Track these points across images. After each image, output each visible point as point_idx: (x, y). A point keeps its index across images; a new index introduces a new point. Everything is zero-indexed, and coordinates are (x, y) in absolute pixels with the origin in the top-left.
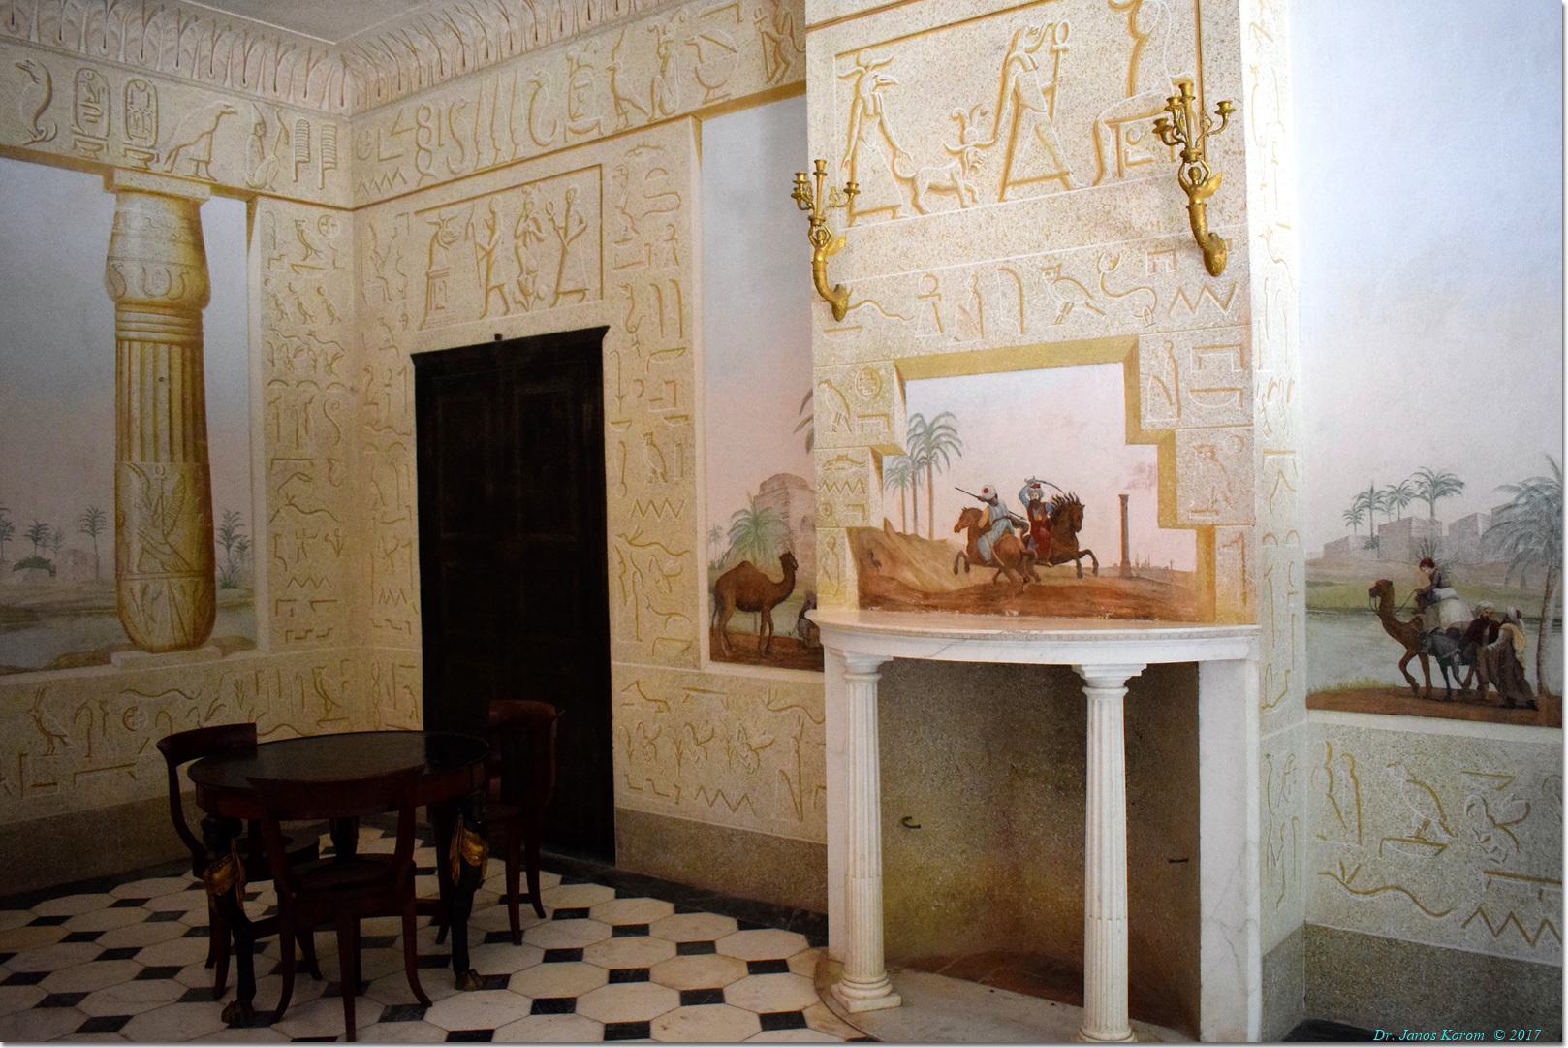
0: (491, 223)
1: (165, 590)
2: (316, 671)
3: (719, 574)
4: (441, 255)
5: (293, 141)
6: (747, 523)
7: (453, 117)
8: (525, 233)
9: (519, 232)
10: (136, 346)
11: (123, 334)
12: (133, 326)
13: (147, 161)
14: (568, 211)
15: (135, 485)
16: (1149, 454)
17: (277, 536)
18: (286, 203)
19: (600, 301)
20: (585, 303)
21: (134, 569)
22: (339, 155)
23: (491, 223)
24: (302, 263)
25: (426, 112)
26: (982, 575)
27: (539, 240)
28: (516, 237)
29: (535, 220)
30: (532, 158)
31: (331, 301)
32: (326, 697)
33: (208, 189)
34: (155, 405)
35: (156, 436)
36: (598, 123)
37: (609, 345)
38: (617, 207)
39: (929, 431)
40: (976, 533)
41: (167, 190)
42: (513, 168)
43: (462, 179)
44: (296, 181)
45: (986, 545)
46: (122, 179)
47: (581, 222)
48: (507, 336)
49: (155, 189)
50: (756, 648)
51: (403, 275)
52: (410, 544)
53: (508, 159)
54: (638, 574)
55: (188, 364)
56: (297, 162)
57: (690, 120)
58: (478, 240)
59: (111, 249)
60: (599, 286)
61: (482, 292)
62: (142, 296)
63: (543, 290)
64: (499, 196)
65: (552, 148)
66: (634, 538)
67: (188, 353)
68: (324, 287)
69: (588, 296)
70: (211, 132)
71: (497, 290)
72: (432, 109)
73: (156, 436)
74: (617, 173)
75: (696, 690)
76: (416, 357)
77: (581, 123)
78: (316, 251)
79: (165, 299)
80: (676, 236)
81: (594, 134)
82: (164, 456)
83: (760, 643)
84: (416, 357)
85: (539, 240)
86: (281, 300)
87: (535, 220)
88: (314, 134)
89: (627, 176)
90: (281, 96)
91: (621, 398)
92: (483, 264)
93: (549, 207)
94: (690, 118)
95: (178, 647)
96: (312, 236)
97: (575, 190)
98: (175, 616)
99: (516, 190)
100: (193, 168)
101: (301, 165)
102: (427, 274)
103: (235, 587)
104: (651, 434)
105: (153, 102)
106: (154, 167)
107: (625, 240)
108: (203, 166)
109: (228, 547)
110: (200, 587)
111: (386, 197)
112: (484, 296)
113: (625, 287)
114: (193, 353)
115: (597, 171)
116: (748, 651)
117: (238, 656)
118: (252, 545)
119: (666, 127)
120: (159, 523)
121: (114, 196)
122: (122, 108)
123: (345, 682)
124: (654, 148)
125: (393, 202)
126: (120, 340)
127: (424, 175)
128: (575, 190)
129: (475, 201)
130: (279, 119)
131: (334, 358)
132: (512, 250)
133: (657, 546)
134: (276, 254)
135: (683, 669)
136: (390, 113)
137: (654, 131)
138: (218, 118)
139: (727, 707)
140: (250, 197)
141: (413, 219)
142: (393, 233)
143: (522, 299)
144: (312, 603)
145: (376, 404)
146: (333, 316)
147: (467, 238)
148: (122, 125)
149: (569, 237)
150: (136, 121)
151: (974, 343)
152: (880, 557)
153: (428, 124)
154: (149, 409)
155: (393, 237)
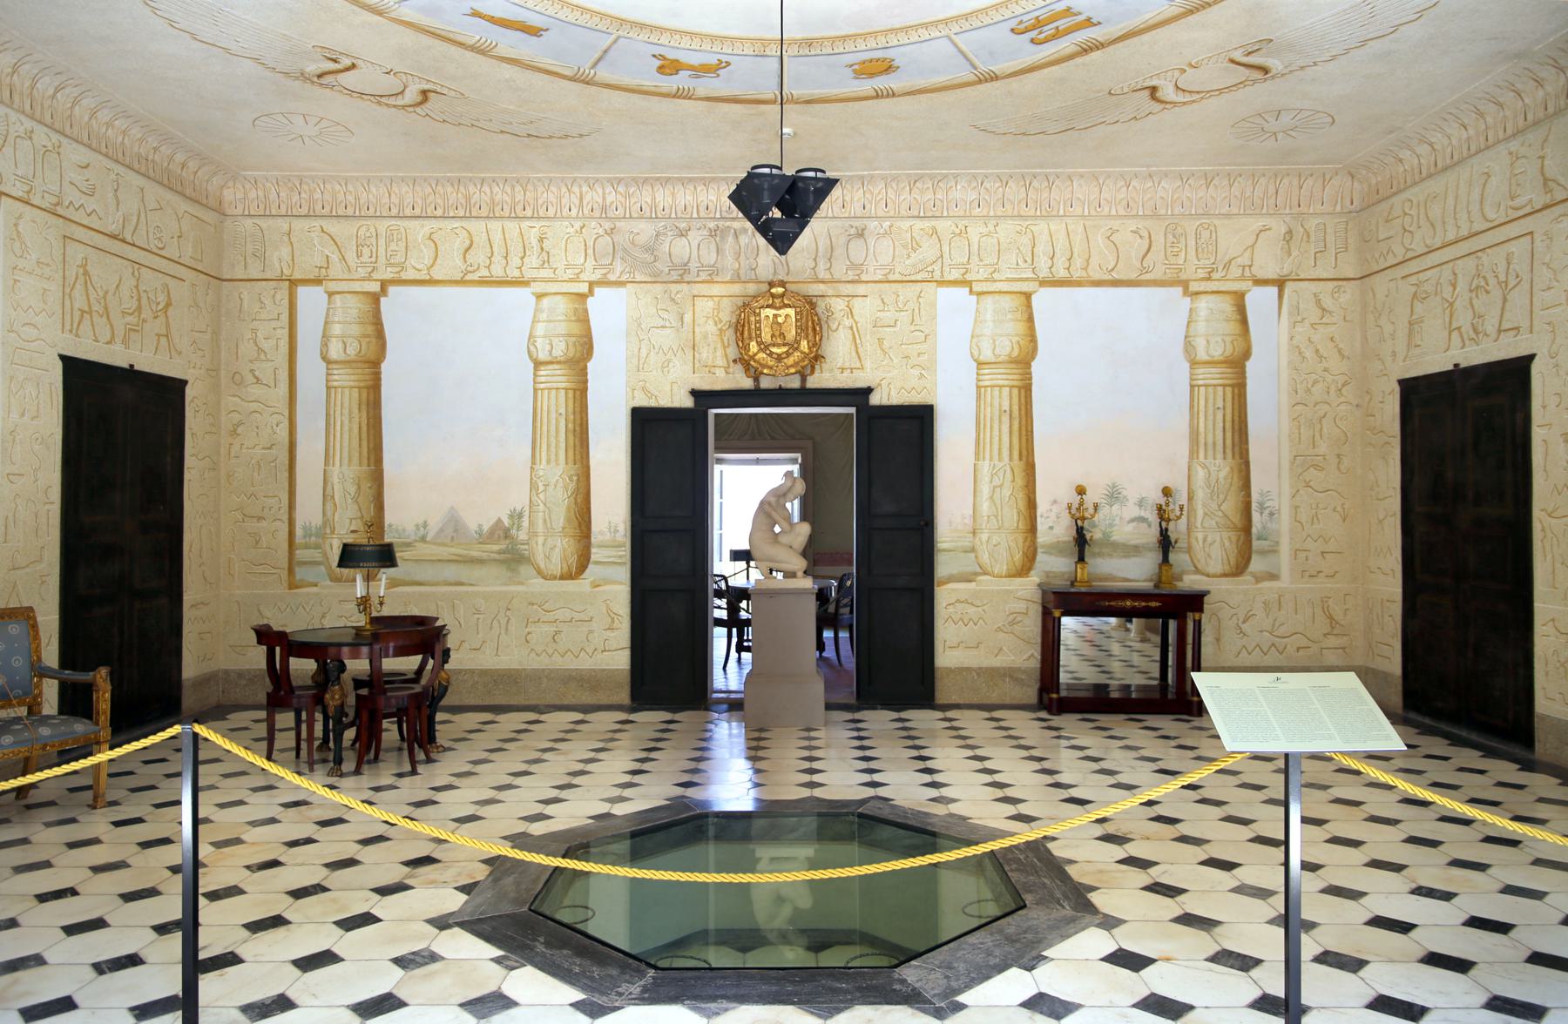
1: (1218, 539)
4: (1419, 307)
5: (1313, 238)
10: (1202, 389)
11: (1195, 383)
12: (1201, 377)
13: (1210, 273)
15: (1200, 474)
17: (1296, 507)
18: (1306, 282)
21: (1199, 525)
22: (1349, 241)
28: (1471, 291)
31: (1340, 346)
32: (1331, 618)
33: (1250, 283)
34: (1214, 425)
35: (1214, 444)
41: (1222, 289)
46: (1194, 287)
49: (1215, 289)
51: (1393, 323)
52: (1395, 514)
55: (1236, 397)
56: (1316, 253)
59: (1187, 331)
61: (1446, 333)
62: (1205, 357)
67: (1236, 391)
70: (1253, 246)
73: (1214, 444)
76: (1401, 382)
78: (1330, 312)
79: (1222, 358)
82: (1219, 455)
84: (1401, 382)
86: (1303, 350)
88: (1328, 230)
90: (1303, 209)
92: (1447, 312)
95: (1225, 575)
96: (1327, 302)
98: (1225, 557)
100: (1240, 271)
102: (1410, 322)
103: (1265, 539)
105: (1214, 235)
106: (1215, 276)
108: (1247, 268)
109: (1262, 513)
110: (1242, 537)
111: (1383, 267)
114: (1239, 390)
117: (1266, 584)
118: (1279, 513)
120: (1215, 498)
121: (1189, 299)
122: (1194, 243)
126: (1192, 386)
127: (1408, 250)
131: (1343, 385)
132: (1468, 301)
134: (1299, 318)
136: (1385, 206)
138: (1258, 235)
140: (1280, 284)
141: (1400, 282)
147: (1436, 294)
148: (1194, 253)
150: (1203, 249)
154: (1210, 427)
155: (1387, 296)
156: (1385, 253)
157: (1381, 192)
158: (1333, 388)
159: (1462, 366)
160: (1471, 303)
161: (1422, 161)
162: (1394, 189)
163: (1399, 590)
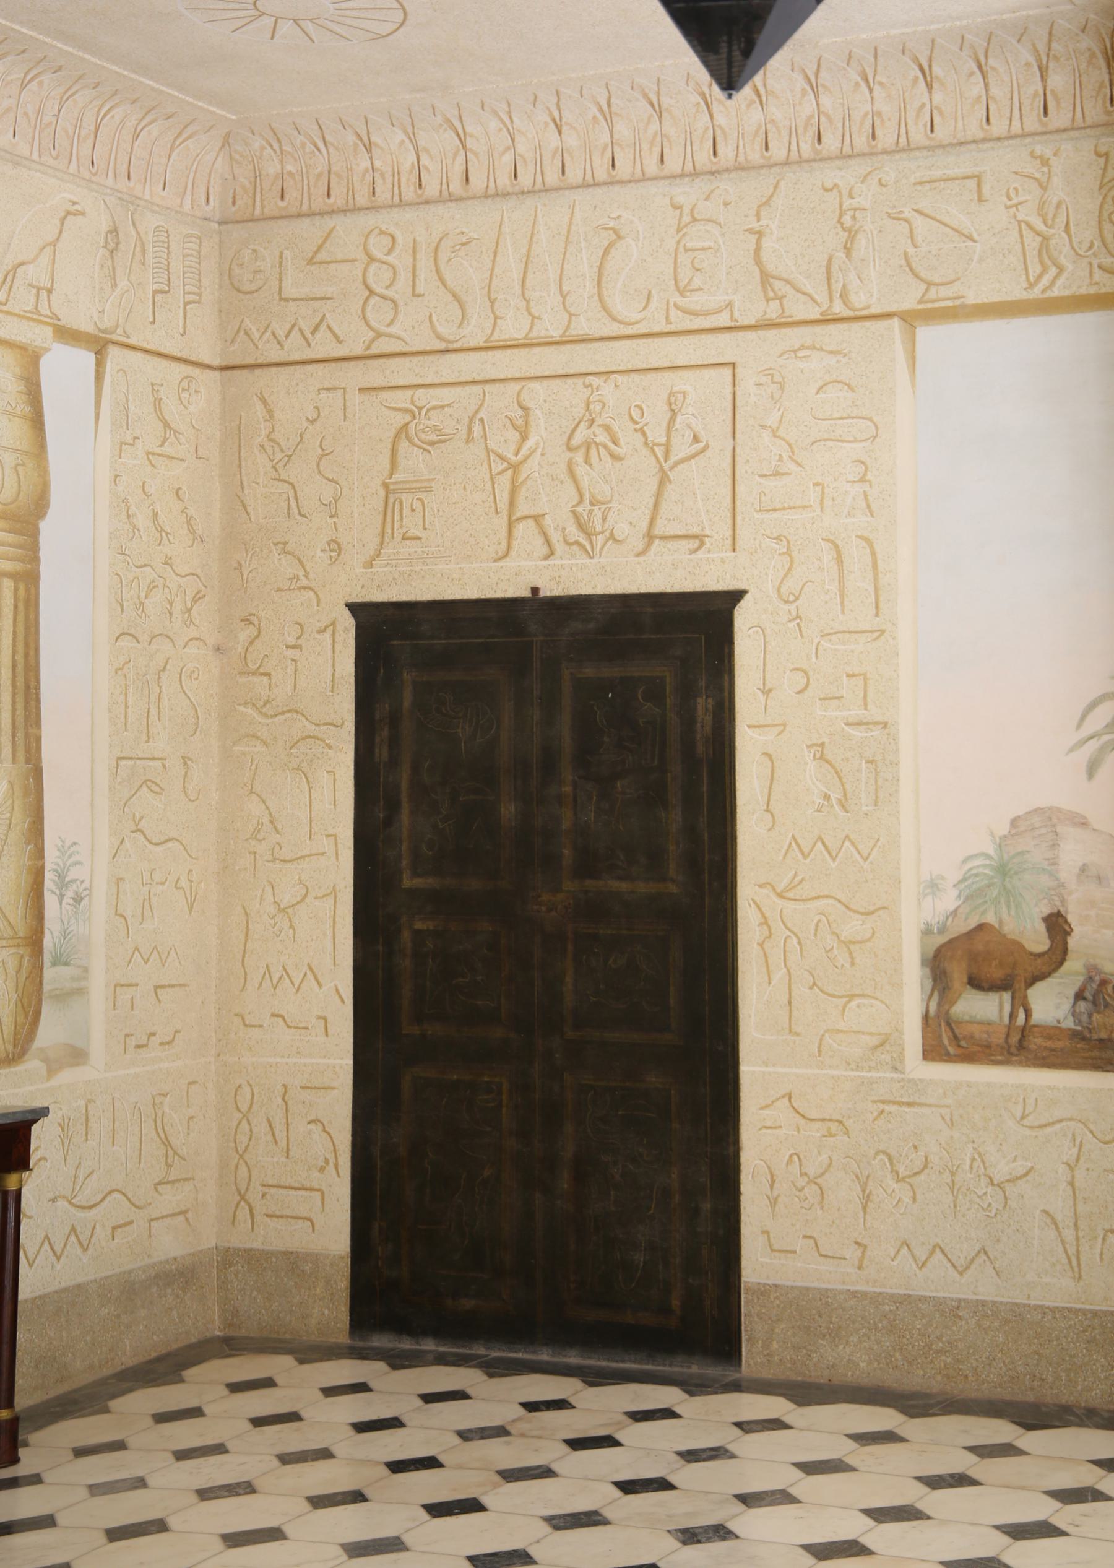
0: (520, 422)
2: (158, 1101)
3: (942, 940)
4: (414, 461)
5: (150, 259)
6: (987, 872)
7: (443, 257)
8: (588, 445)
9: (575, 442)
14: (672, 419)
18: (140, 355)
19: (731, 554)
20: (700, 554)
22: (205, 282)
23: (520, 422)
24: (158, 450)
25: (387, 241)
27: (615, 457)
29: (607, 428)
30: (601, 339)
31: (191, 511)
32: (167, 1143)
36: (730, 305)
37: (743, 617)
38: (763, 427)
42: (563, 348)
43: (455, 351)
44: (154, 322)
47: (696, 439)
48: (549, 590)
50: (1001, 1041)
51: (332, 481)
53: (556, 334)
54: (795, 940)
56: (155, 292)
57: (896, 322)
58: (492, 445)
60: (729, 533)
61: (502, 523)
63: (622, 529)
64: (535, 385)
65: (641, 329)
66: (788, 889)
68: (184, 488)
69: (708, 545)
71: (531, 523)
72: (398, 235)
74: (764, 379)
75: (894, 1103)
76: (356, 609)
77: (694, 301)
78: (175, 431)
80: (868, 477)
81: (723, 320)
83: (1008, 1035)
84: (356, 609)
85: (615, 457)
86: (133, 510)
87: (607, 428)
89: (781, 387)
91: (767, 692)
92: (504, 481)
93: (635, 414)
94: (896, 320)
97: (685, 394)
99: (570, 381)
101: (159, 297)
102: (386, 486)
104: (822, 745)
107: (777, 474)
111: (296, 357)
112: (505, 528)
113: (778, 539)
115: (727, 372)
116: (988, 1047)
119: (856, 326)
123: (192, 1118)
124: (831, 352)
125: (309, 368)
127: (379, 335)
128: (685, 394)
129: (487, 388)
130: (134, 224)
131: (195, 600)
132: (563, 466)
133: (830, 901)
135: (874, 1074)
136: (309, 231)
137: (832, 328)
139: (952, 1124)
142: (312, 415)
143: (582, 539)
144: (156, 987)
145: (269, 675)
146: (193, 533)
147: (469, 439)
149: (673, 459)
153: (390, 259)
156: (306, 326)
157: (292, 194)
158: (178, 608)
159: (542, 594)
160: (571, 473)
161: (424, 161)
162: (338, 198)
163: (347, 1062)
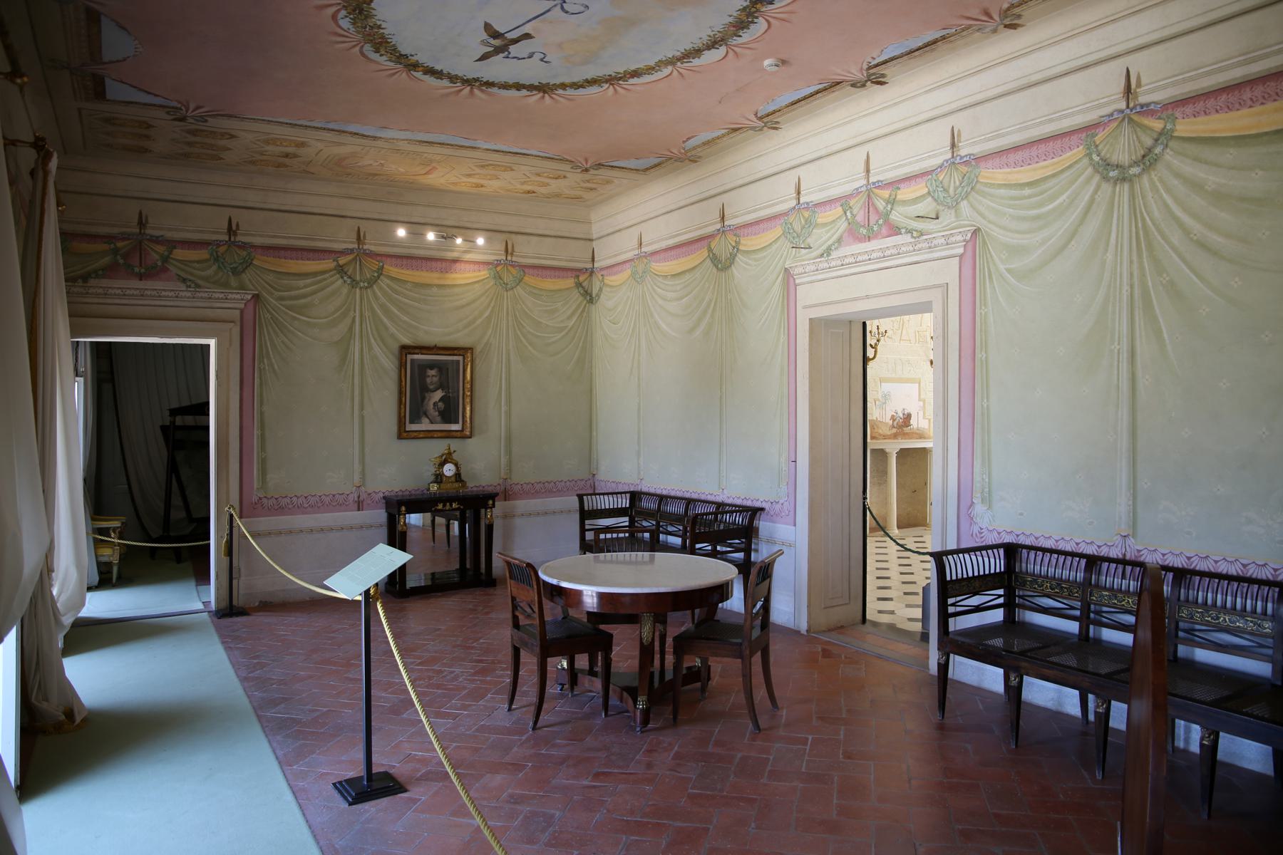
16: (921, 403)
26: (894, 431)
39: (886, 395)
40: (894, 420)
45: (895, 423)
151: (894, 375)
152: (875, 427)
